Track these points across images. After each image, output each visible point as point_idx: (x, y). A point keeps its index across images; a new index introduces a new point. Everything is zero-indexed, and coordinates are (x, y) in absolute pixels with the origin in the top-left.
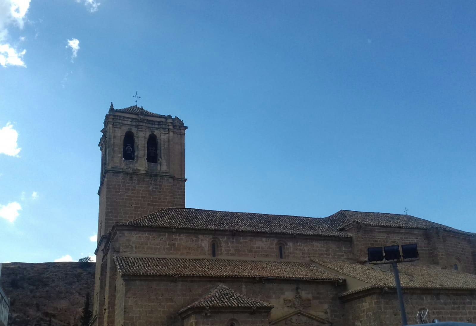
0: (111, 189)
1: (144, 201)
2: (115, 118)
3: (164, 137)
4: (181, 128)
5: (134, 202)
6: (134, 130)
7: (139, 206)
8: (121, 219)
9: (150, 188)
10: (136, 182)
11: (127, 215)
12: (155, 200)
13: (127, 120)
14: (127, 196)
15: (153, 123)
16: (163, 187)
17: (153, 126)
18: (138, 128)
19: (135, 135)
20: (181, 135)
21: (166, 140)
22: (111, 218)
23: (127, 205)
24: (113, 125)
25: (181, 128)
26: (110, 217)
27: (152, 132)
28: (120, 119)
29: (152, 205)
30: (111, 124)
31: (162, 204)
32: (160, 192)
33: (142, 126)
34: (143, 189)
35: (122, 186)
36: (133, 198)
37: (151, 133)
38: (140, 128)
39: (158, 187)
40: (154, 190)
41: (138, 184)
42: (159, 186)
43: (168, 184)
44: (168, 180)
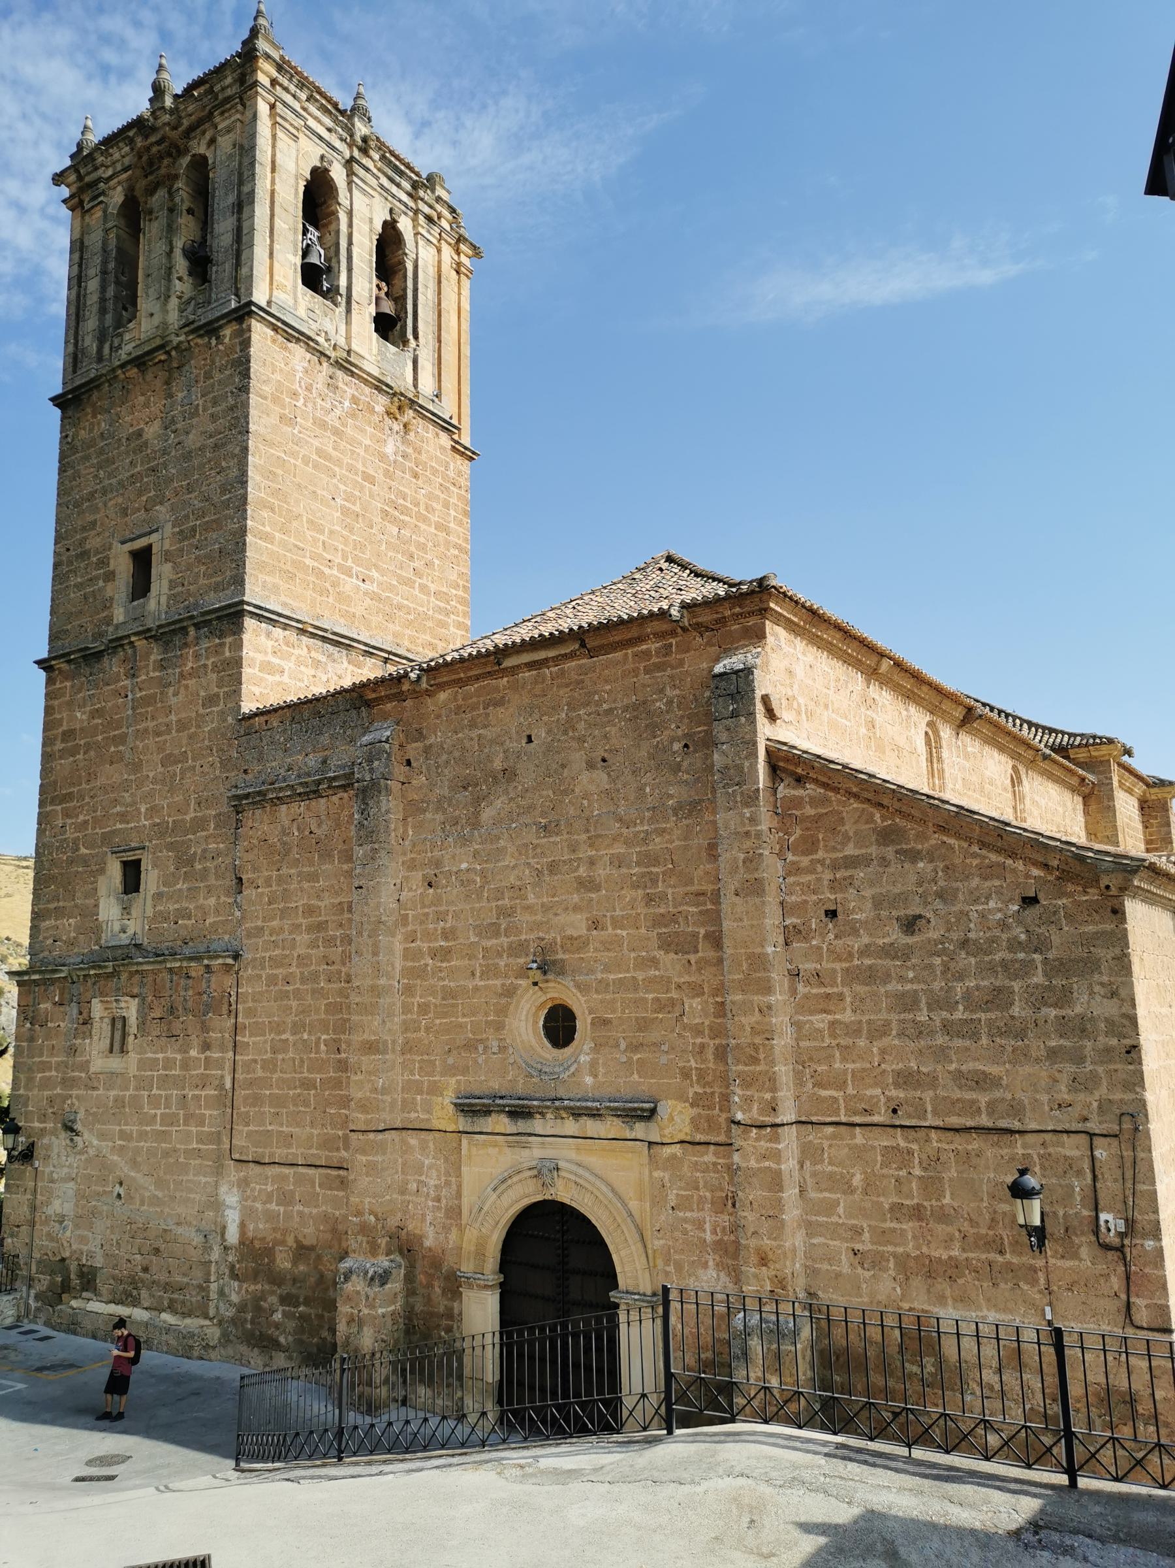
0: (265, 398)
1: (371, 496)
2: (281, 79)
3: (427, 255)
4: (462, 247)
5: (342, 487)
6: (338, 174)
7: (357, 508)
8: (301, 545)
9: (389, 449)
10: (347, 404)
11: (322, 537)
12: (401, 501)
13: (318, 114)
14: (319, 452)
15: (397, 179)
16: (424, 457)
17: (394, 189)
18: (351, 173)
19: (343, 196)
20: (458, 272)
21: (432, 271)
22: (268, 529)
23: (319, 492)
24: (273, 107)
25: (462, 247)
26: (263, 525)
27: (391, 211)
28: (294, 96)
29: (394, 521)
30: (264, 99)
31: (423, 526)
32: (416, 476)
33: (367, 169)
34: (368, 442)
35: (302, 401)
36: (337, 469)
37: (389, 218)
38: (357, 176)
39: (410, 451)
40: (400, 459)
41: (353, 416)
42: (415, 449)
43: (438, 454)
44: (437, 434)
